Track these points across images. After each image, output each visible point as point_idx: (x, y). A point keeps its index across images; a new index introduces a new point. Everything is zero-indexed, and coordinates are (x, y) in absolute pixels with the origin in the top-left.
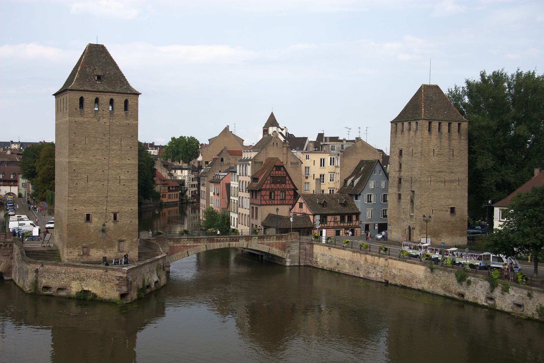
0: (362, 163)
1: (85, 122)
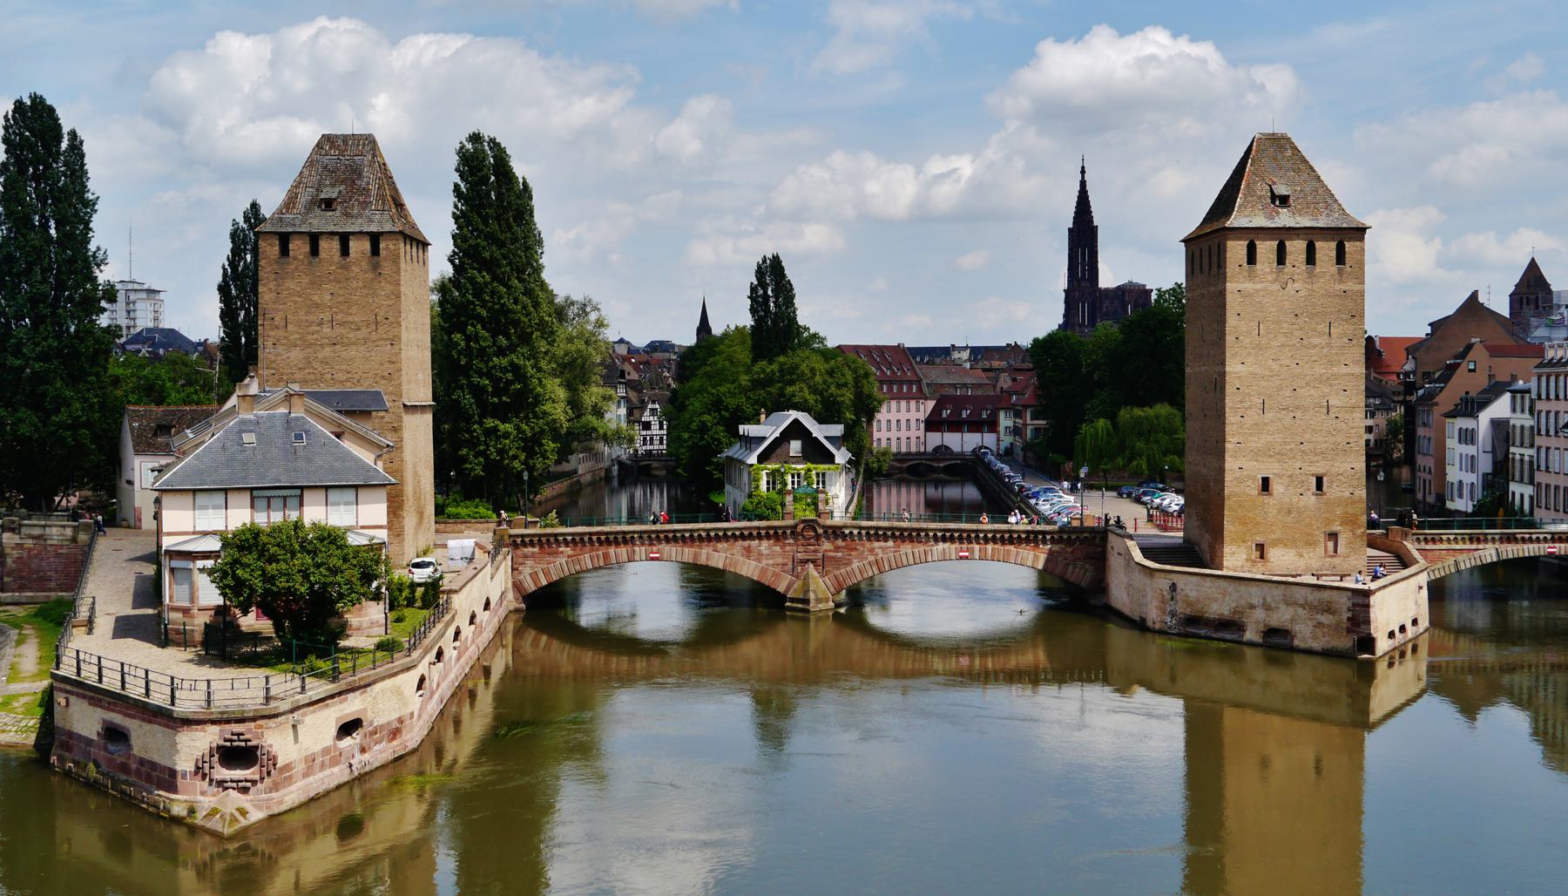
1: (1258, 291)
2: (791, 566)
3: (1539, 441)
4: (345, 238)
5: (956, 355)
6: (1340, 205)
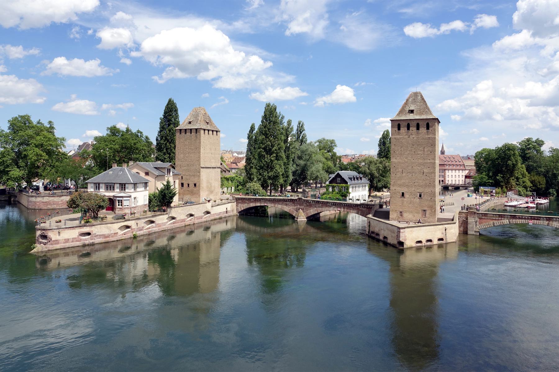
4: (191, 130)
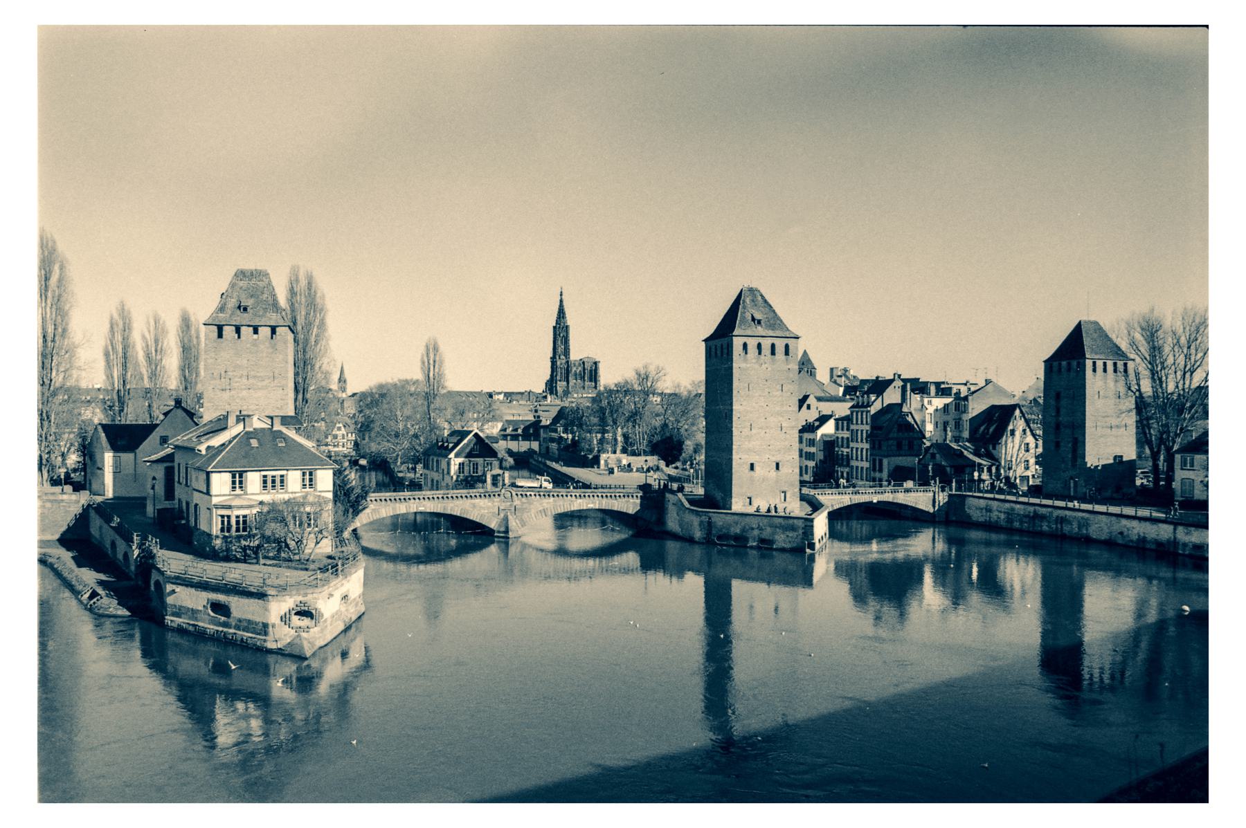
0: (993, 407)
2: (497, 512)
3: (852, 445)
5: (496, 397)
6: (785, 325)
